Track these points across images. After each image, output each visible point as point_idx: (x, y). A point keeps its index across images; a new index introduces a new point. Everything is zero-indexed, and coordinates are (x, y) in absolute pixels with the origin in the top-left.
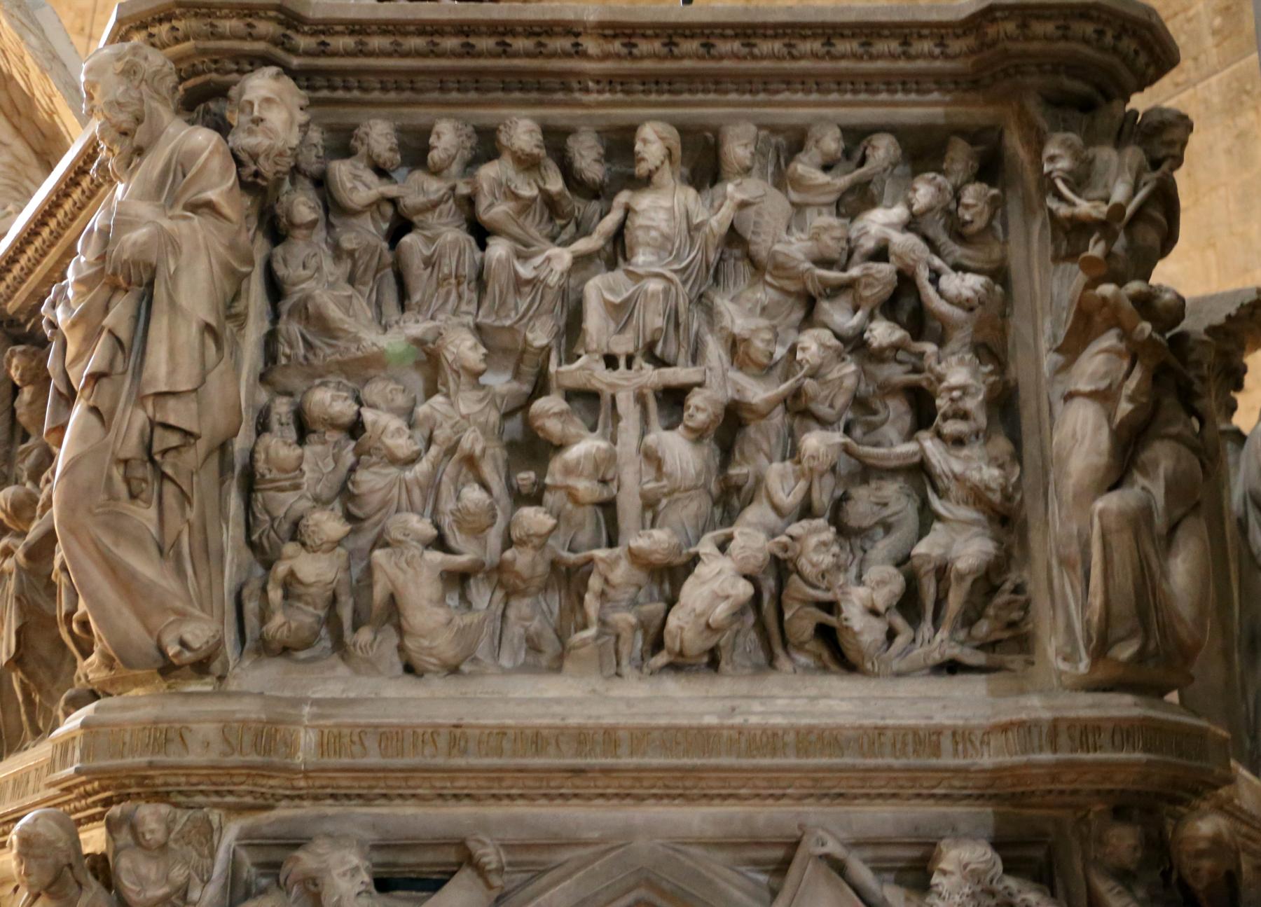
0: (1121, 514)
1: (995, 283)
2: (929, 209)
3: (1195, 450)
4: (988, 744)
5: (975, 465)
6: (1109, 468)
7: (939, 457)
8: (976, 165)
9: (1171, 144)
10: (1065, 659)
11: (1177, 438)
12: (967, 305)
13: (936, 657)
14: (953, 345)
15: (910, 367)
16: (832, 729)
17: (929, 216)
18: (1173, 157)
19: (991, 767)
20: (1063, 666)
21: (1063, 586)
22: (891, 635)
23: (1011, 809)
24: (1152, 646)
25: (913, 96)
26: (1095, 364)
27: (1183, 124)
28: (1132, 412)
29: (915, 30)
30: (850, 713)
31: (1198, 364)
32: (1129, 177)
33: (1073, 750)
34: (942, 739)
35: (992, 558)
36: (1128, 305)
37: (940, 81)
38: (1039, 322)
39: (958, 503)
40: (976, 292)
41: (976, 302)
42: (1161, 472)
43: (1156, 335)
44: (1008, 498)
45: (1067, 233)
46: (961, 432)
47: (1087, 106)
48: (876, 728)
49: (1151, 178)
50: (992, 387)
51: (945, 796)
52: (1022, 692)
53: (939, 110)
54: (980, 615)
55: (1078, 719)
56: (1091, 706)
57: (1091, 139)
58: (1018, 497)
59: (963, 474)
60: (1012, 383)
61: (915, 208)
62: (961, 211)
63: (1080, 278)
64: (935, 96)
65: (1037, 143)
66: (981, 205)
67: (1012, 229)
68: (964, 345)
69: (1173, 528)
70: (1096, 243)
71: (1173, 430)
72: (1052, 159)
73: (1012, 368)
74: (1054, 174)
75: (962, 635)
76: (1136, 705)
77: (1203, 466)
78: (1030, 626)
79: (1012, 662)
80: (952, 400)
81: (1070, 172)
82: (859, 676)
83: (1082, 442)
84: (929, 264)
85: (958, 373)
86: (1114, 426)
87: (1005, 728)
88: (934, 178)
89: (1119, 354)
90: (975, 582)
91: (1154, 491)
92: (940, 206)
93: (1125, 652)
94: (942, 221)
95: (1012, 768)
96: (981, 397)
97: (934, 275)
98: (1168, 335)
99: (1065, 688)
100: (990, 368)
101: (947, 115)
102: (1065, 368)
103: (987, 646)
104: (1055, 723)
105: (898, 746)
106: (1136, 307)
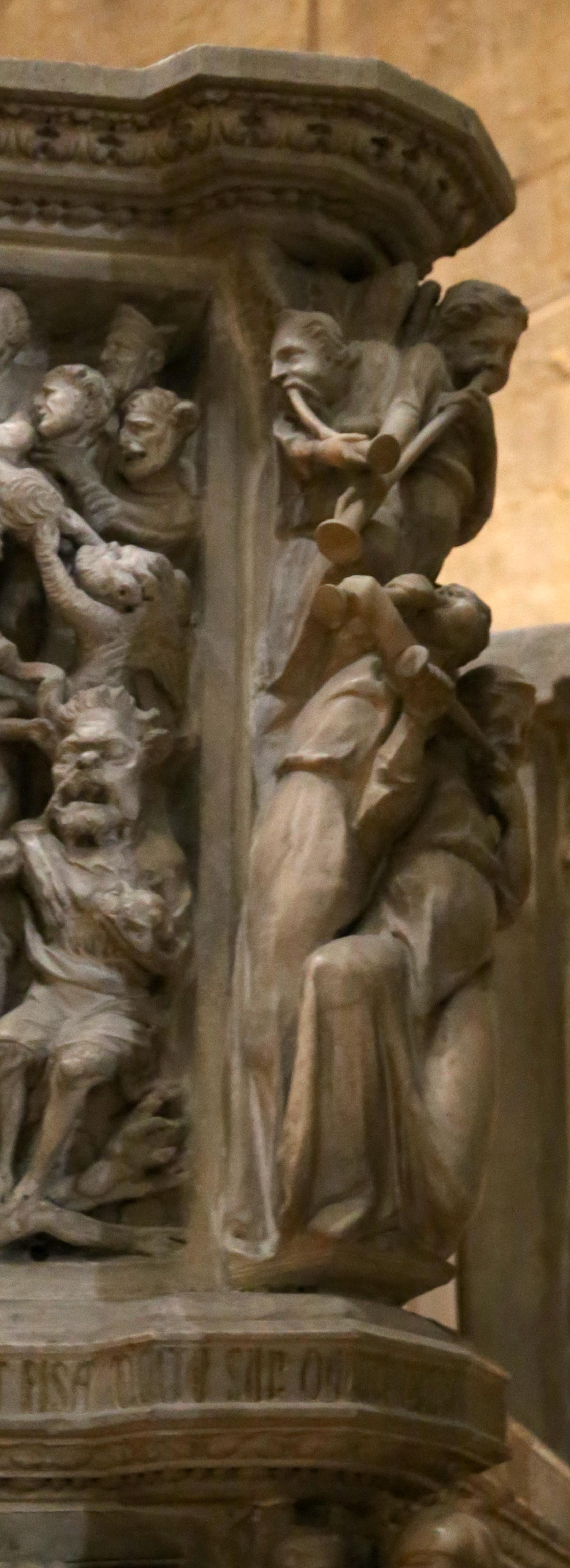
0: (354, 976)
1: (176, 565)
2: (69, 429)
3: (489, 873)
4: (86, 1384)
5: (112, 884)
6: (341, 897)
7: (49, 868)
8: (160, 358)
9: (488, 345)
10: (238, 1235)
11: (461, 850)
12: (119, 600)
13: (14, 1226)
14: (92, 671)
15: (11, 706)
17: (67, 441)
18: (491, 367)
20: (234, 1246)
21: (246, 1107)
23: (121, 1508)
24: (386, 1211)
25: (57, 228)
26: (332, 716)
27: (514, 313)
28: (386, 800)
29: (65, 109)
31: (505, 724)
32: (413, 397)
33: (231, 1396)
35: (127, 1049)
36: (391, 613)
37: (104, 204)
38: (247, 642)
39: (77, 951)
40: (138, 577)
41: (137, 599)
42: (428, 906)
43: (435, 669)
44: (164, 944)
45: (305, 485)
46: (91, 823)
47: (356, 271)
49: (451, 399)
50: (153, 748)
52: (160, 1291)
53: (102, 256)
54: (99, 1153)
55: (246, 1339)
56: (271, 1317)
57: (357, 327)
58: (183, 944)
59: (88, 899)
60: (191, 744)
61: (45, 423)
62: (126, 435)
63: (319, 563)
64: (96, 231)
65: (264, 327)
66: (161, 426)
67: (212, 475)
68: (111, 672)
69: (440, 1006)
70: (348, 503)
71: (453, 835)
72: (287, 355)
73: (194, 718)
74: (288, 382)
75: (62, 1189)
76: (349, 1315)
77: (500, 899)
78: (185, 1175)
79: (146, 1238)
80: (81, 766)
81: (315, 379)
83: (299, 850)
84: (61, 525)
85: (95, 719)
86: (355, 824)
87: (116, 1355)
88: (82, 374)
89: (373, 698)
90: (93, 1093)
91: (412, 940)
92: (89, 424)
93: (339, 1220)
94: (92, 452)
95: (128, 1426)
96: (131, 764)
97: (68, 547)
98: (463, 671)
99: (233, 1284)
100: (153, 712)
101: (115, 266)
102: (281, 722)
103: (105, 1210)
104: (206, 1344)
106: (405, 620)
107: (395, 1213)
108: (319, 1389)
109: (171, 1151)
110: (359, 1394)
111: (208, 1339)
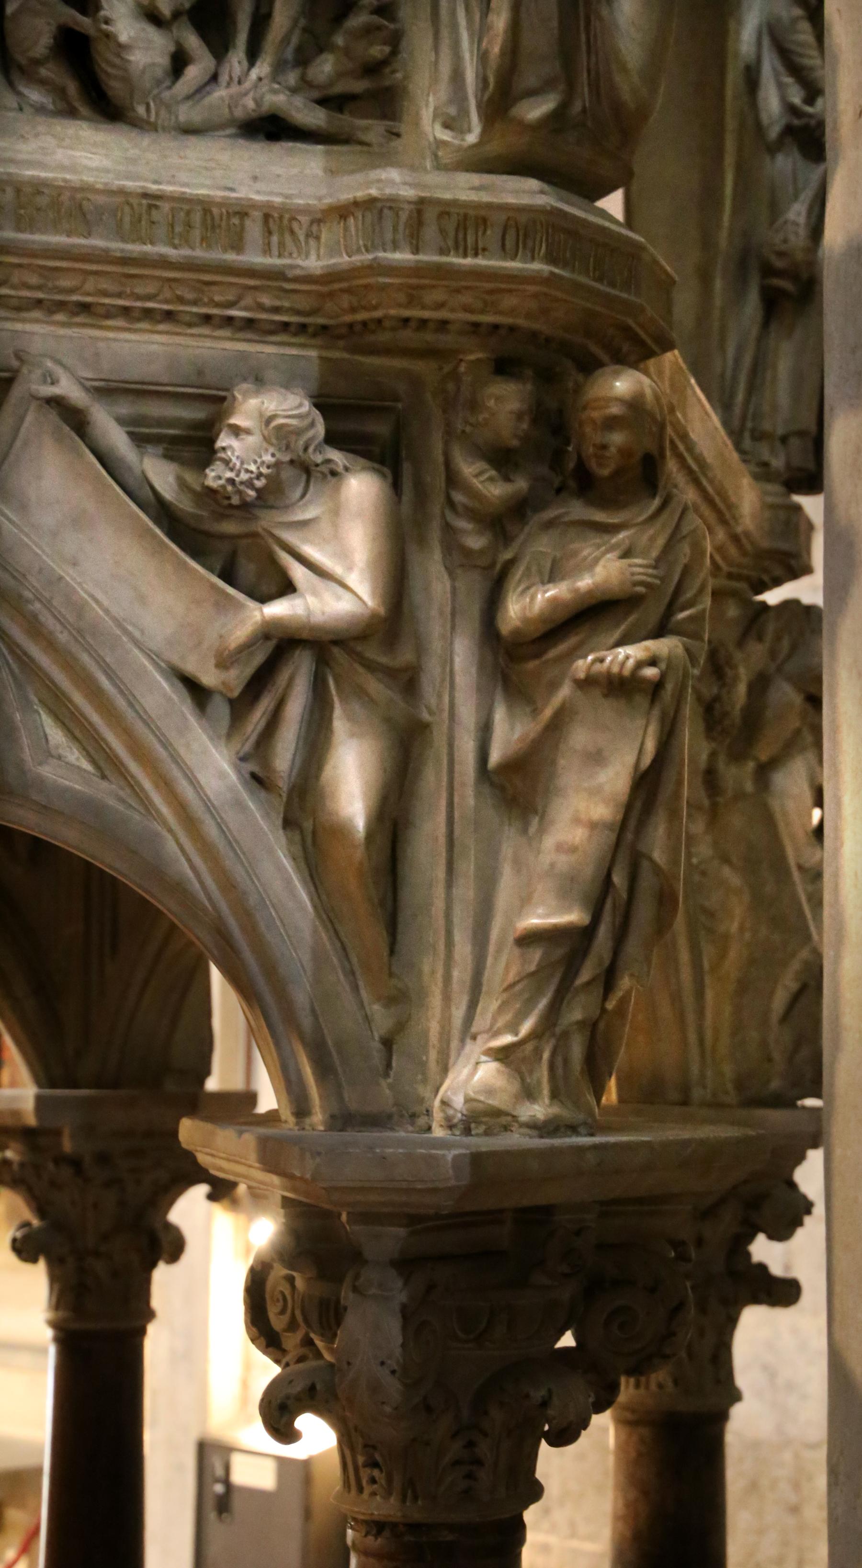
4: (318, 238)
10: (447, 126)
16: (75, 190)
19: (319, 272)
22: (179, 61)
23: (346, 356)
24: (577, 107)
30: (107, 171)
33: (443, 252)
34: (248, 222)
48: (145, 195)
51: (249, 324)
55: (455, 203)
75: (292, 78)
76: (542, 192)
78: (399, 75)
79: (367, 129)
82: (126, 128)
87: (343, 212)
93: (535, 110)
104: (422, 202)
105: (178, 229)
107: (584, 110)
108: (516, 255)
109: (387, 49)
110: (551, 259)
111: (422, 201)
